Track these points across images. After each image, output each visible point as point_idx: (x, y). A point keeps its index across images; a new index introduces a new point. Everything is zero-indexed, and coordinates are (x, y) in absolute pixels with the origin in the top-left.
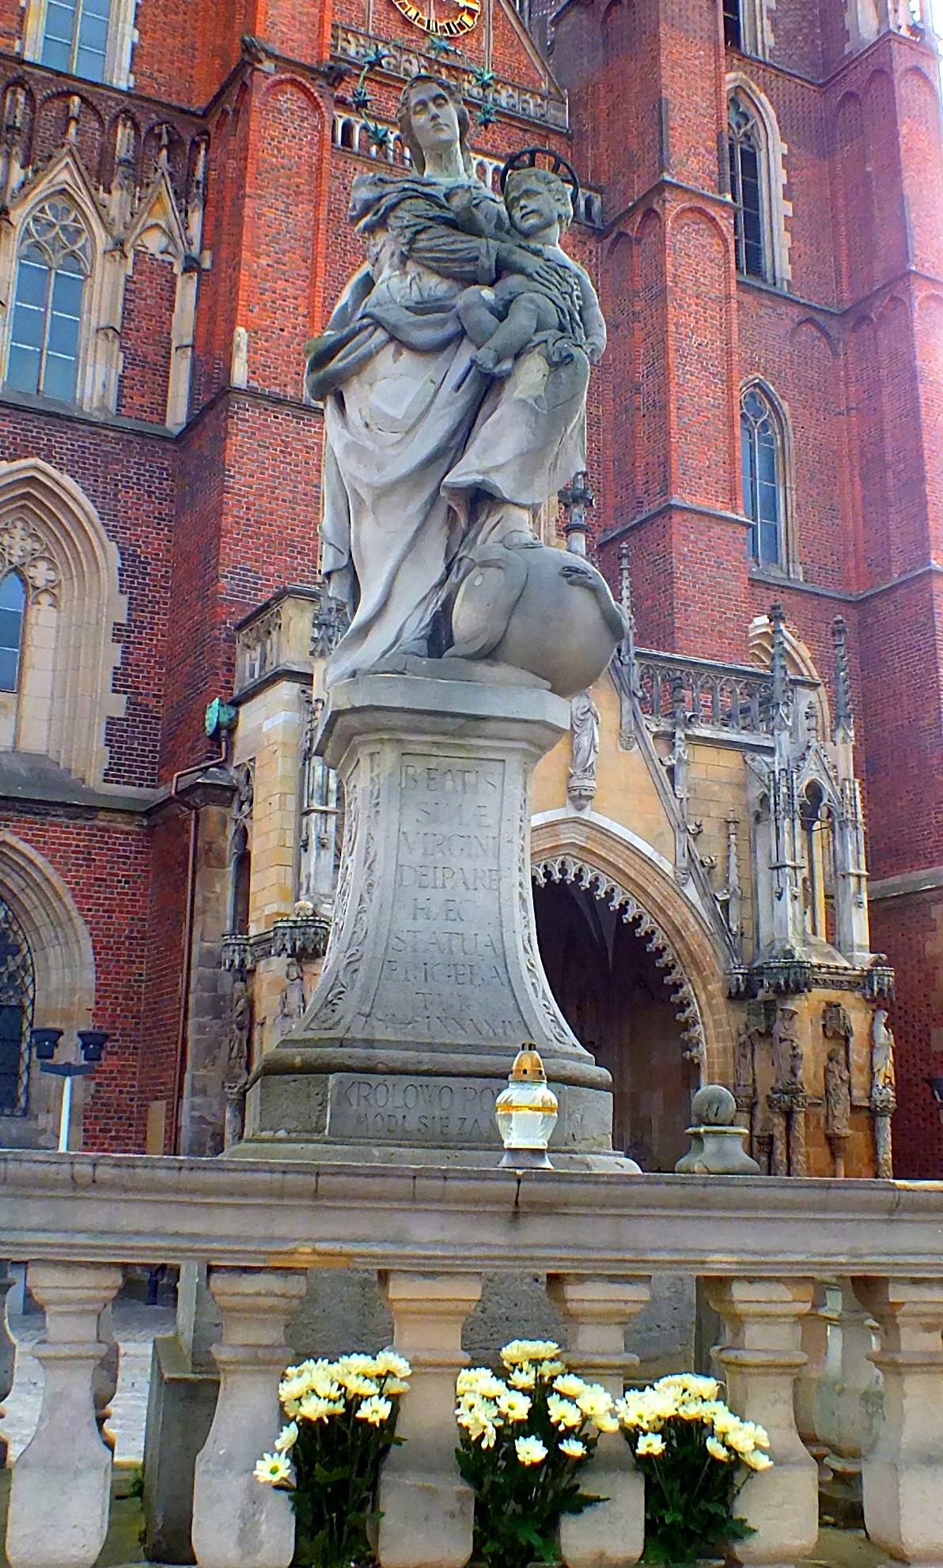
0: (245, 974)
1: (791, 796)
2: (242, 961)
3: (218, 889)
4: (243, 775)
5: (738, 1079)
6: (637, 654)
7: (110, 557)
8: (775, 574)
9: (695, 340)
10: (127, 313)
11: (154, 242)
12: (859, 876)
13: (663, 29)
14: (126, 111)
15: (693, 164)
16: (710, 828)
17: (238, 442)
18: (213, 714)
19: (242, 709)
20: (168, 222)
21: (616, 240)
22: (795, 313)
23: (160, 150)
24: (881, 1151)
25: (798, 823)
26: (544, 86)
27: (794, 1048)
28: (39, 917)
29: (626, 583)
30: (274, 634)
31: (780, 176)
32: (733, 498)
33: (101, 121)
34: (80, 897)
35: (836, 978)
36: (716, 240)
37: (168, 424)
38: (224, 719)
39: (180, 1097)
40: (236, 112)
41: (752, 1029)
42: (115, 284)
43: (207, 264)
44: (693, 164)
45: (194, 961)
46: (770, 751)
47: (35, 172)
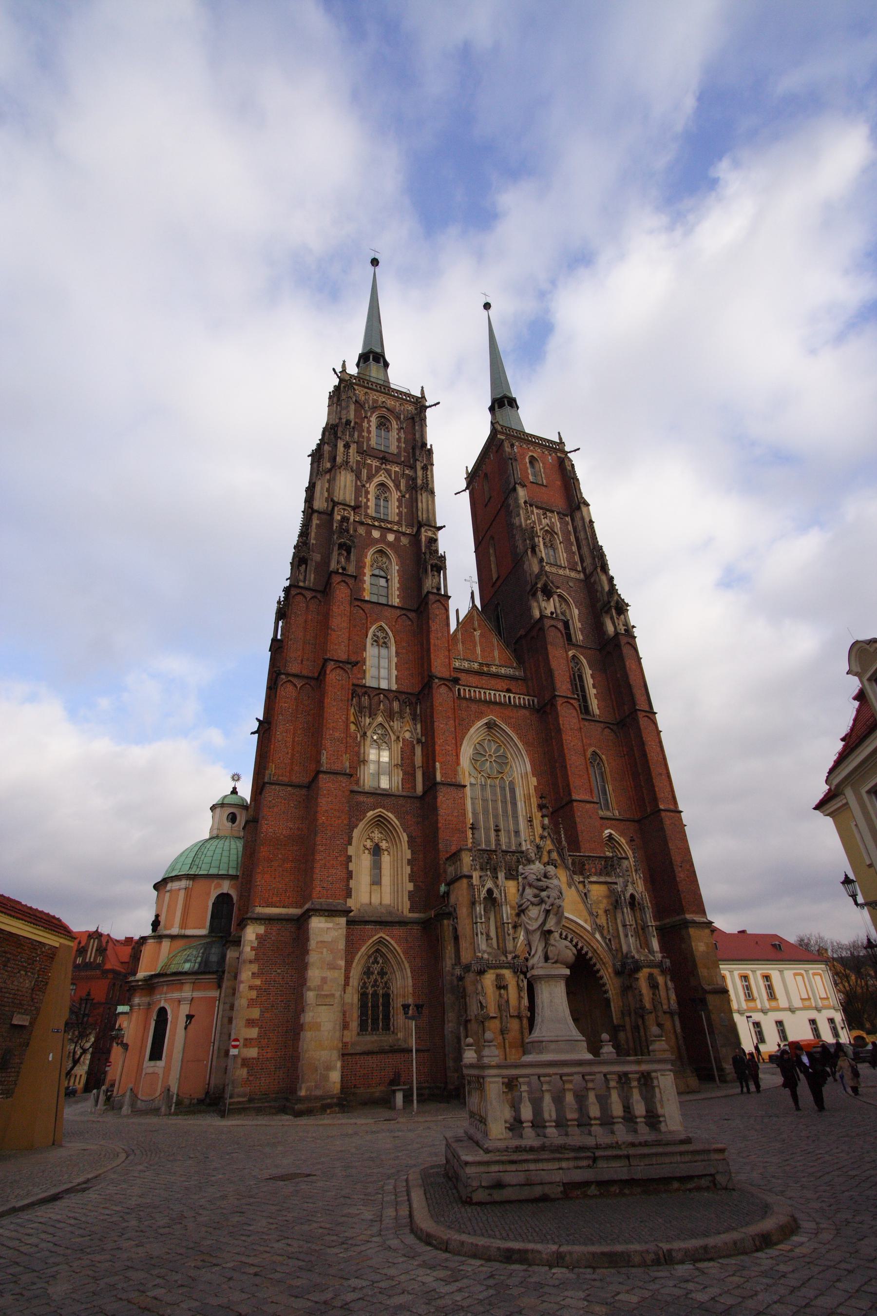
0: (461, 978)
1: (625, 899)
6: (570, 855)
7: (405, 837)
8: (609, 814)
9: (572, 744)
10: (402, 759)
11: (407, 735)
12: (652, 926)
13: (549, 647)
16: (601, 912)
17: (441, 798)
18: (443, 888)
22: (602, 725)
26: (515, 665)
28: (393, 961)
30: (458, 863)
32: (591, 792)
33: (389, 700)
34: (405, 953)
36: (575, 711)
38: (446, 890)
42: (397, 750)
43: (424, 741)
46: (616, 883)
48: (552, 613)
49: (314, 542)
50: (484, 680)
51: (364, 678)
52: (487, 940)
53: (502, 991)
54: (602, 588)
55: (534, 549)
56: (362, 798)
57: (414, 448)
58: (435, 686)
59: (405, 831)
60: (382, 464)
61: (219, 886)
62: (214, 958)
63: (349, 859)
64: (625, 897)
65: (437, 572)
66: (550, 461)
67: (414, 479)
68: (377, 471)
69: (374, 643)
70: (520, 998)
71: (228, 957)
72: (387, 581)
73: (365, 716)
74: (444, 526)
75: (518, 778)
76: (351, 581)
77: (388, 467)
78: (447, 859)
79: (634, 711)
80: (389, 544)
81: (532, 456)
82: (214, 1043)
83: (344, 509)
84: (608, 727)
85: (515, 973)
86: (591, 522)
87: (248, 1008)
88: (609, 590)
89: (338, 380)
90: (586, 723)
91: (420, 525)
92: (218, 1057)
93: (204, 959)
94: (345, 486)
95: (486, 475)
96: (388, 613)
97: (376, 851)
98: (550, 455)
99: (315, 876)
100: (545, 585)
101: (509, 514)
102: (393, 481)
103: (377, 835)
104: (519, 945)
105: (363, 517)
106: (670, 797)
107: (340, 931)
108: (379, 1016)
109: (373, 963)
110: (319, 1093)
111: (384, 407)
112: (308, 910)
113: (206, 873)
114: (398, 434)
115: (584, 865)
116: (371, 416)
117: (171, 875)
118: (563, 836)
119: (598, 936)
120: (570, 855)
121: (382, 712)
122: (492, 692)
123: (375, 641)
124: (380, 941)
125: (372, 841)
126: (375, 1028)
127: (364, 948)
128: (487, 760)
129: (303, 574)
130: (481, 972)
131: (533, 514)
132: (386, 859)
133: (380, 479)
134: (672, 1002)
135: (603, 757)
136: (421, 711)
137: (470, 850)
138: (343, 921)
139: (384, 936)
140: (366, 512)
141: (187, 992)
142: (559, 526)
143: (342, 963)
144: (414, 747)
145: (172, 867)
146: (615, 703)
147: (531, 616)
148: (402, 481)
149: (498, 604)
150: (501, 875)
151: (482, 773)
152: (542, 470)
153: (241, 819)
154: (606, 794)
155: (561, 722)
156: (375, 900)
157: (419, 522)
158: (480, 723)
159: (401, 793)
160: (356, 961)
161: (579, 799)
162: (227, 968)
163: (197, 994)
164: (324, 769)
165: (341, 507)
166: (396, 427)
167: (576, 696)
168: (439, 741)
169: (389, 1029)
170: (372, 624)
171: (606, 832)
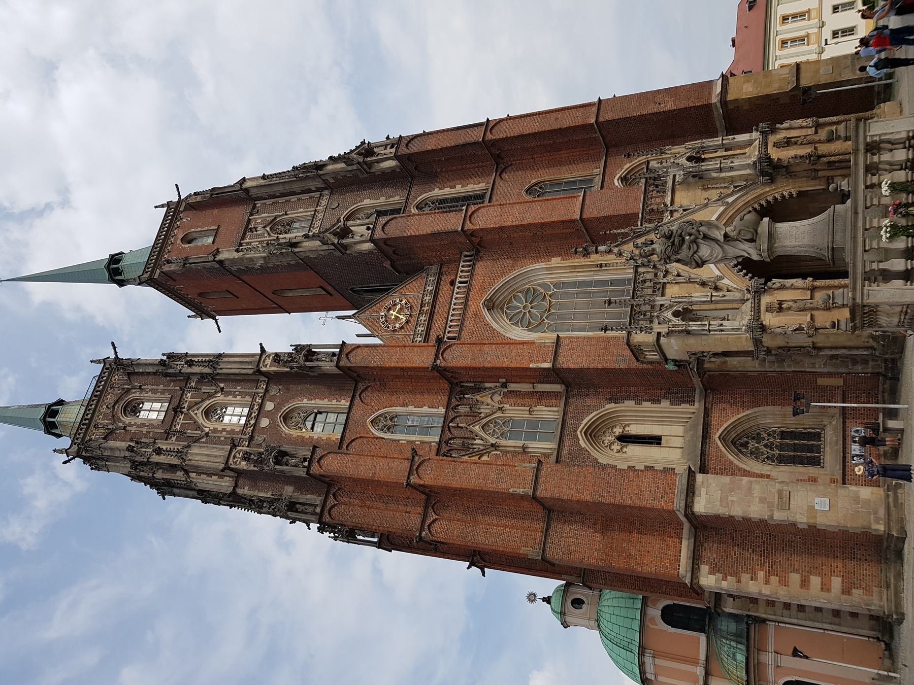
0: (769, 351)
2: (764, 351)
3: (735, 363)
4: (693, 356)
5: (804, 177)
7: (611, 406)
8: (598, 180)
9: (517, 215)
12: (723, 140)
14: (452, 409)
15: (453, 221)
18: (671, 367)
19: (668, 358)
20: (489, 394)
21: (480, 246)
23: (464, 397)
24: (833, 121)
25: (703, 164)
26: (423, 275)
27: (792, 158)
28: (746, 426)
29: (615, 231)
31: (447, 190)
33: (457, 417)
35: (763, 144)
36: (480, 211)
37: (561, 391)
38: (672, 363)
39: (816, 372)
40: (452, 372)
41: (785, 173)
43: (504, 380)
44: (453, 221)
45: (764, 370)
46: (674, 176)
47: (477, 436)
48: (368, 229)
49: (270, 493)
50: (440, 309)
51: (430, 443)
52: (728, 320)
53: (784, 306)
54: (342, 170)
55: (294, 245)
56: (565, 452)
57: (166, 375)
58: (443, 364)
59: (604, 406)
60: (182, 413)
61: (653, 620)
62: (733, 627)
63: (632, 468)
64: (690, 167)
65: (313, 356)
66: (189, 219)
67: (203, 376)
68: (191, 418)
69: (391, 430)
70: (792, 287)
71: (732, 611)
72: (320, 413)
73: (473, 444)
74: (261, 344)
75: (551, 278)
76: (319, 453)
77: (186, 405)
78: (638, 361)
79: (486, 144)
80: (277, 408)
81: (182, 240)
82: (824, 629)
83: (234, 457)
84: (500, 175)
85: (765, 291)
86: (264, 177)
87: (788, 586)
88: (344, 162)
89: (77, 459)
90: (494, 198)
91: (259, 372)
92: (839, 625)
93: (732, 638)
94: (206, 455)
95: (200, 295)
96: (357, 412)
97: (625, 439)
98: (182, 219)
99: (649, 506)
100: (335, 234)
101: (249, 270)
102: (203, 401)
103: (609, 438)
104: (736, 286)
105: (243, 437)
106: (582, 110)
107: (710, 481)
108: (804, 444)
109: (746, 447)
110: (882, 512)
111: (113, 406)
112: (686, 515)
113: (637, 634)
114: (147, 393)
115: (652, 209)
116: (124, 423)
117: (639, 675)
118: (619, 231)
119: (730, 200)
120: (641, 225)
121: (469, 425)
122: (454, 301)
123: (389, 429)
124: (722, 438)
125: (612, 443)
126: (818, 449)
127: (730, 457)
128: (529, 312)
129: (307, 507)
130: (763, 328)
131: (251, 243)
132: (635, 429)
133: (199, 415)
134: (805, 124)
135: (533, 181)
136: (473, 382)
137: (629, 334)
138: (700, 477)
139: (718, 435)
140: (238, 433)
141: (768, 658)
142: (266, 215)
143: (745, 479)
144: (511, 392)
145: (629, 673)
146: (473, 165)
147: (370, 252)
148: (203, 391)
149: (351, 290)
150: (660, 300)
151: (544, 317)
152: (199, 229)
153: (580, 592)
154: (576, 181)
155: (492, 226)
156: (679, 442)
157: (254, 373)
158: (488, 318)
159: (562, 409)
160: (744, 466)
161: (579, 211)
162: (745, 613)
163: (771, 647)
164: (531, 493)
165: (231, 461)
166: (138, 394)
167: (464, 208)
168: (506, 363)
169: (819, 434)
170: (369, 432)
171: (617, 184)
